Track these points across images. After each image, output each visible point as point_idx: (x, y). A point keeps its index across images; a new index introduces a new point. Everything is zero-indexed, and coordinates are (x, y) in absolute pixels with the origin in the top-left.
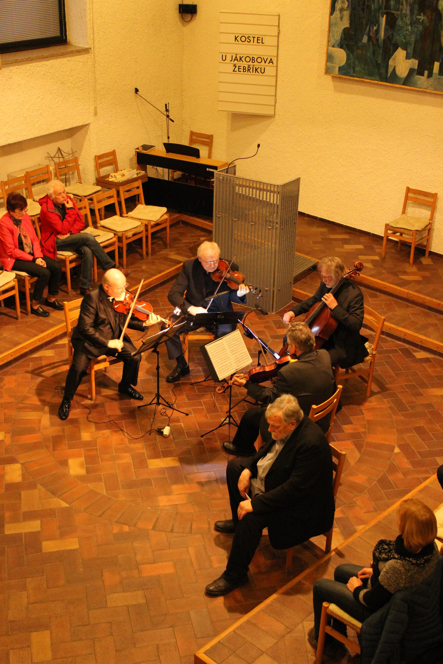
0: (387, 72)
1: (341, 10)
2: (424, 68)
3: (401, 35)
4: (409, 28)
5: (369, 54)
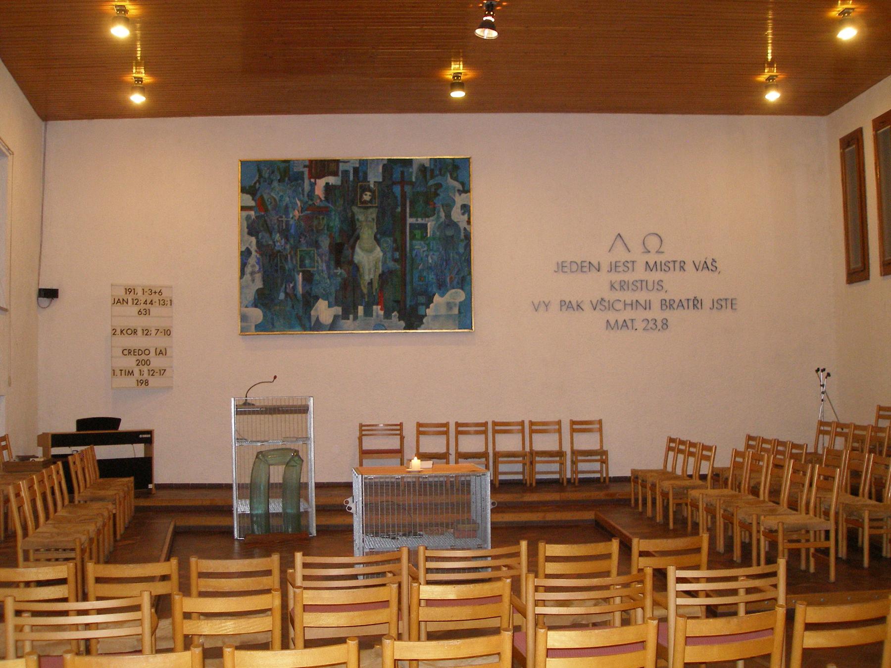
0: (310, 321)
1: (252, 273)
2: (348, 311)
4: (328, 281)
5: (288, 308)
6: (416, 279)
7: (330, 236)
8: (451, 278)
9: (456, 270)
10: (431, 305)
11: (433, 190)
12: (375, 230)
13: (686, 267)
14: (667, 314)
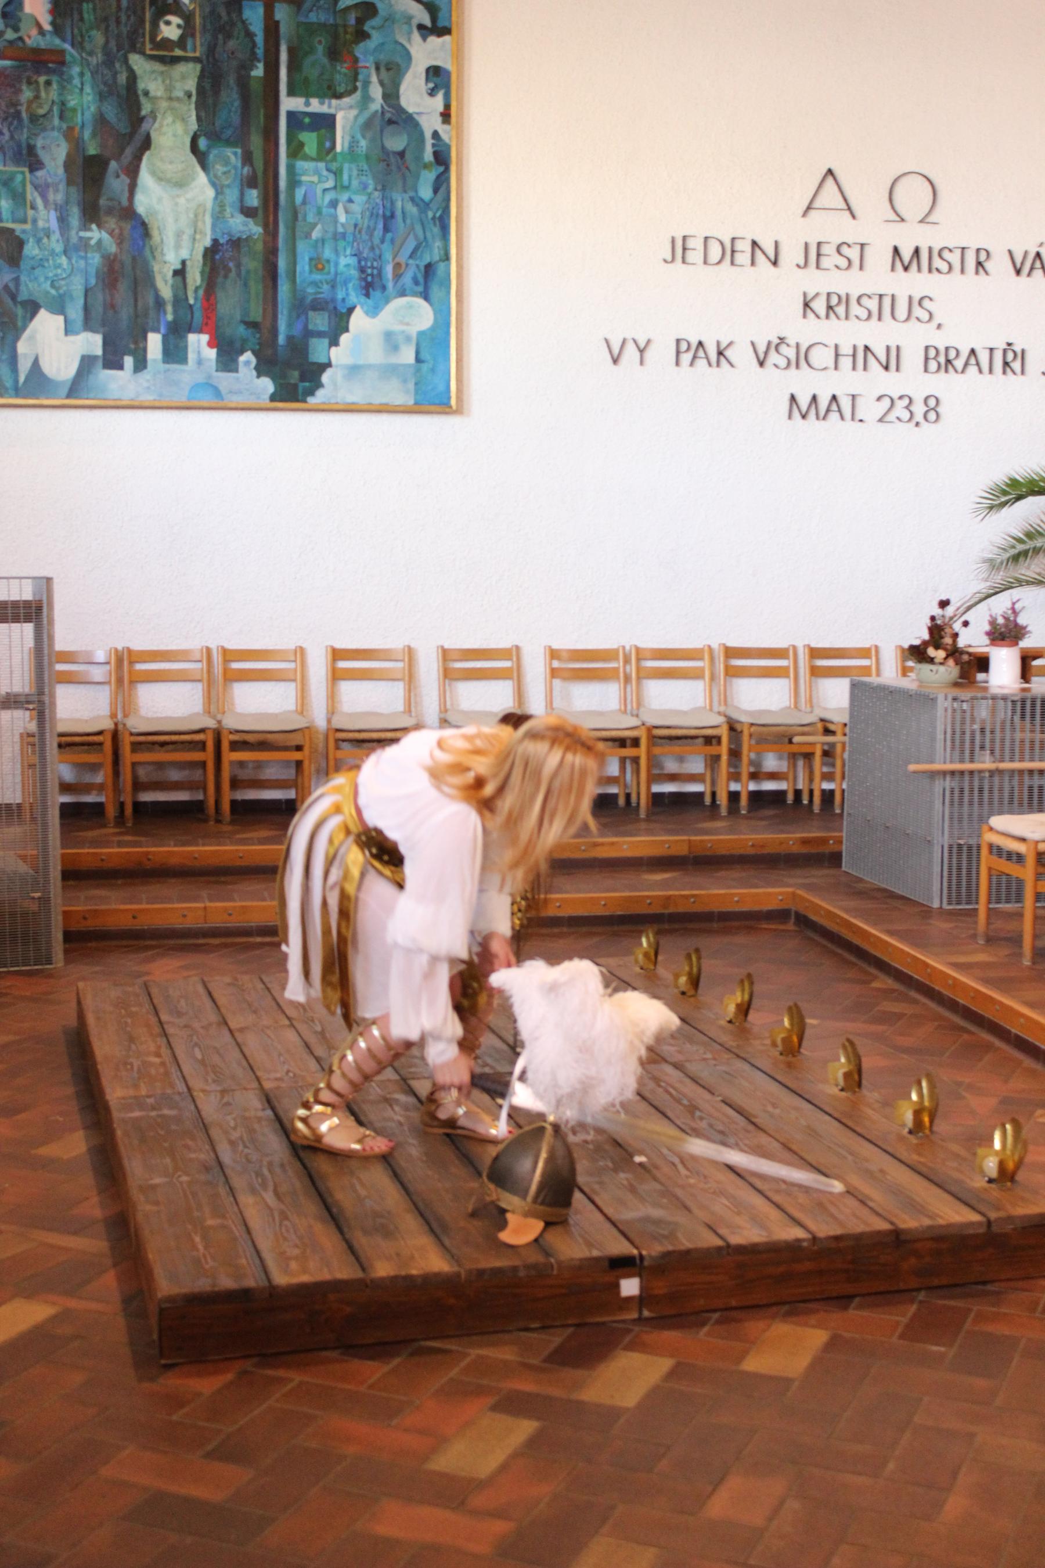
2: (121, 347)
3: (42, 279)
4: (64, 260)
6: (303, 266)
7: (69, 134)
8: (397, 266)
9: (411, 244)
10: (344, 338)
11: (352, 19)
12: (194, 126)
13: (988, 265)
14: (939, 384)
